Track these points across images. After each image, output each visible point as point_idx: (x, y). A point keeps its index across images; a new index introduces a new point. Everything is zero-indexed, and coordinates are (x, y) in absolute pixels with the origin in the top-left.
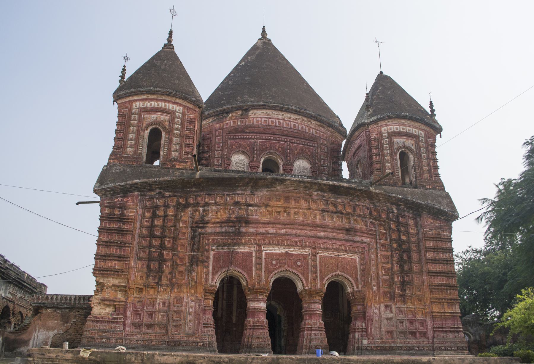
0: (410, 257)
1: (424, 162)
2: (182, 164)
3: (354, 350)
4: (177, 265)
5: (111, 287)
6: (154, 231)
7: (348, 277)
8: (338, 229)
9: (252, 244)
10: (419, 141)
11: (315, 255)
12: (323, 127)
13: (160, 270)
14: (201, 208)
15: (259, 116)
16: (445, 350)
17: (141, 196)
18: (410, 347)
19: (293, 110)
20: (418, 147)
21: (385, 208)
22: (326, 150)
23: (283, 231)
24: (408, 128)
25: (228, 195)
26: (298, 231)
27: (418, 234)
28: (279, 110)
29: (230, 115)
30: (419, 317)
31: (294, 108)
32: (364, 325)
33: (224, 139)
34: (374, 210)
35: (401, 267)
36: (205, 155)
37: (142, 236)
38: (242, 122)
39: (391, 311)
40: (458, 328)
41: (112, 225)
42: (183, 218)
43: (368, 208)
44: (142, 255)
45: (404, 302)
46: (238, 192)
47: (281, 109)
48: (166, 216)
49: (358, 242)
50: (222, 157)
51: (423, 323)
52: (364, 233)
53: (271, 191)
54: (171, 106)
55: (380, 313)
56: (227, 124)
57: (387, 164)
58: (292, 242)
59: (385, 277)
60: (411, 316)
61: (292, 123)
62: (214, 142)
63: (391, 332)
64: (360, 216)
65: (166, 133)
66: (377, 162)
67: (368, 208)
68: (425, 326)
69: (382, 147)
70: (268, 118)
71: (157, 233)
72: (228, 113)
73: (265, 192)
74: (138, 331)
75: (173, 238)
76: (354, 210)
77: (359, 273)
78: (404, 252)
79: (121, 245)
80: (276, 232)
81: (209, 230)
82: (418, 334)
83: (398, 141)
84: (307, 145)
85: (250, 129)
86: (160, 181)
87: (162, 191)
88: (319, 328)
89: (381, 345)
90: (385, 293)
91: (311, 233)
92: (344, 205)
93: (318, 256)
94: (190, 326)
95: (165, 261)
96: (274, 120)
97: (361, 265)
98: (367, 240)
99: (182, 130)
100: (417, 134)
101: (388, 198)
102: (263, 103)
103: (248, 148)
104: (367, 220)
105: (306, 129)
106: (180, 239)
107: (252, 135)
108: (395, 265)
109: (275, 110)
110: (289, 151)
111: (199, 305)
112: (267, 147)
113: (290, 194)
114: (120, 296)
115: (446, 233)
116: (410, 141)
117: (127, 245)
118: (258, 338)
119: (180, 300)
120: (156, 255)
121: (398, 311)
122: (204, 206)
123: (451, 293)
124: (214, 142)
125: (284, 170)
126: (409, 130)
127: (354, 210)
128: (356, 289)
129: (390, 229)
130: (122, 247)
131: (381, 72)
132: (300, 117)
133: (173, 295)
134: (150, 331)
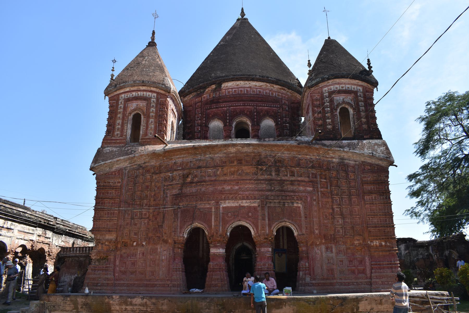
1: (363, 114)
12: (284, 90)
16: (383, 284)
18: (349, 283)
22: (287, 109)
24: (348, 86)
28: (246, 80)
29: (207, 90)
32: (307, 264)
33: (202, 110)
36: (188, 125)
50: (200, 126)
55: (322, 253)
56: (204, 97)
57: (327, 120)
62: (194, 114)
65: (144, 115)
68: (363, 263)
72: (205, 88)
83: (339, 98)
96: (243, 89)
99: (156, 113)
100: (356, 90)
102: (232, 77)
103: (222, 115)
107: (224, 104)
111: (170, 254)
112: (237, 113)
126: (348, 88)
131: (329, 38)
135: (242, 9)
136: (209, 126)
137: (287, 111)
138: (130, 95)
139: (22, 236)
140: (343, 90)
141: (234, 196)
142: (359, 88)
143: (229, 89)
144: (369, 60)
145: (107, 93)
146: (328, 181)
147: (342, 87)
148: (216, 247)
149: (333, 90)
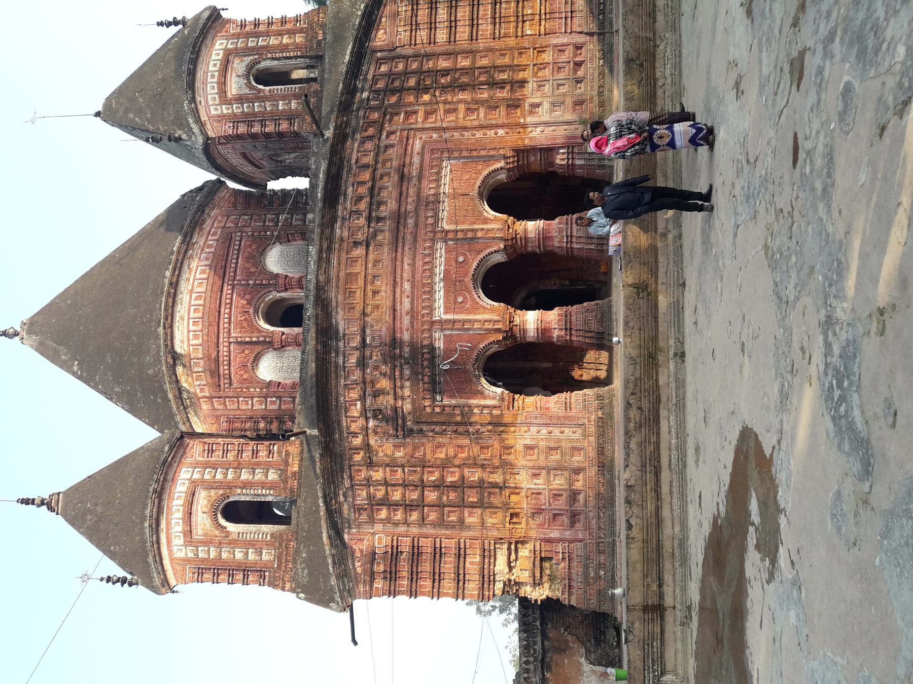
1: (273, 41)
2: (290, 460)
3: (604, 166)
5: (511, 568)
6: (412, 501)
7: (481, 178)
8: (401, 194)
9: (431, 337)
10: (236, 49)
12: (204, 221)
13: (481, 485)
14: (371, 423)
16: (604, 13)
17: (350, 528)
18: (600, 73)
19: (173, 275)
23: (407, 286)
27: (404, 57)
29: (185, 385)
33: (231, 394)
34: (366, 131)
35: (463, 88)
38: (197, 364)
41: (405, 574)
44: (453, 518)
45: (523, 83)
47: (173, 296)
49: (422, 161)
50: (266, 397)
52: (406, 149)
53: (337, 307)
57: (280, 108)
59: (482, 115)
61: (198, 276)
62: (238, 412)
64: (377, 155)
67: (362, 143)
69: (247, 114)
70: (189, 319)
71: (415, 496)
72: (180, 390)
73: (340, 317)
74: (582, 517)
76: (366, 166)
80: (408, 297)
81: (408, 407)
84: (239, 250)
85: (211, 350)
86: (325, 497)
87: (341, 492)
88: (567, 224)
91: (409, 237)
92: (359, 183)
93: (446, 227)
94: (571, 434)
95: (463, 478)
96: (192, 308)
98: (418, 145)
102: (161, 328)
103: (247, 352)
104: (382, 145)
105: (209, 253)
106: (425, 454)
107: (221, 347)
108: (460, 97)
109: (173, 306)
110: (250, 282)
112: (245, 319)
113: (342, 274)
116: (235, 65)
117: (438, 545)
118: (586, 322)
120: (453, 496)
121: (539, 94)
122: (367, 419)
124: (238, 412)
125: (286, 290)
126: (215, 65)
128: (502, 164)
129: (398, 104)
130: (441, 554)
133: (521, 462)
134: (581, 497)
136: (268, 380)
137: (251, 219)
140: (219, 76)
143: (188, 337)
146: (404, 109)
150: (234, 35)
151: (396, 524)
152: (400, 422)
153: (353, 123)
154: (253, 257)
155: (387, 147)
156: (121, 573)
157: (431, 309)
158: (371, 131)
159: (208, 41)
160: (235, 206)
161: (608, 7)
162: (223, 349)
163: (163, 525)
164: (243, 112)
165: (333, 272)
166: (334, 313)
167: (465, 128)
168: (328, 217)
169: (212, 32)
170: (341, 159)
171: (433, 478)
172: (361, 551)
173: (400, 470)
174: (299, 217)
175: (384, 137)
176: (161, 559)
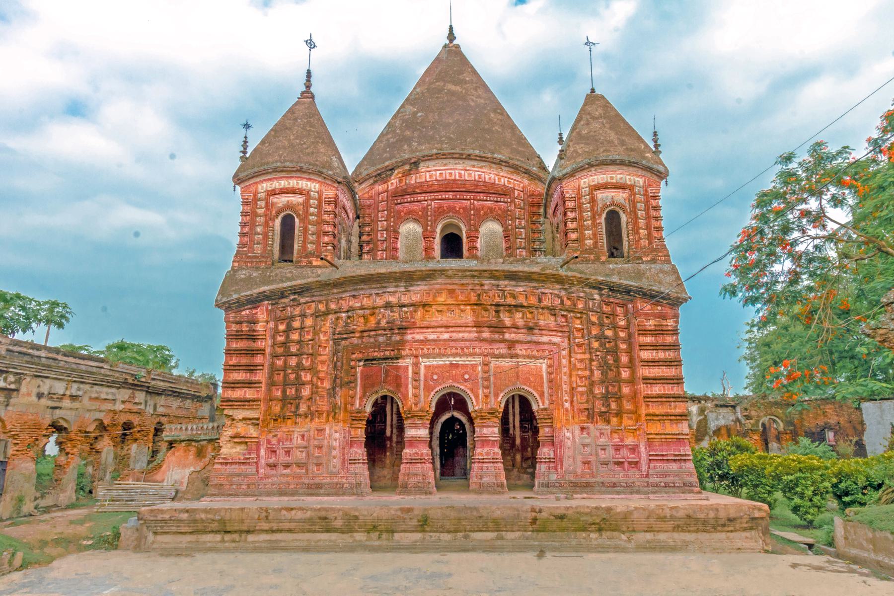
0: (617, 360)
1: (642, 223)
4: (317, 387)
6: (289, 348)
7: (531, 390)
9: (407, 356)
10: (634, 194)
11: (486, 364)
12: (518, 174)
13: (298, 397)
14: (344, 315)
15: (432, 172)
17: (272, 304)
20: (633, 203)
21: (582, 295)
23: (446, 336)
25: (377, 294)
26: (466, 335)
27: (628, 325)
29: (396, 172)
30: (629, 441)
31: (477, 152)
34: (568, 299)
36: (367, 229)
37: (275, 356)
39: (588, 434)
40: (686, 455)
42: (323, 329)
43: (559, 297)
45: (608, 422)
46: (389, 290)
47: (461, 157)
48: (302, 328)
49: (544, 344)
50: (386, 230)
51: (634, 449)
54: (303, 184)
55: (574, 437)
58: (457, 349)
59: (580, 389)
60: (616, 440)
61: (477, 173)
63: (588, 463)
64: (548, 308)
66: (574, 230)
67: (559, 297)
71: (294, 349)
73: (422, 287)
74: (273, 472)
75: (312, 355)
76: (540, 300)
77: (546, 385)
78: (608, 352)
79: (251, 368)
81: (355, 341)
82: (626, 465)
84: (497, 201)
89: (574, 480)
90: (581, 411)
97: (550, 374)
98: (556, 340)
101: (585, 283)
106: (320, 355)
108: (596, 372)
111: (344, 437)
113: (454, 287)
114: (253, 432)
115: (670, 322)
116: (621, 194)
118: (416, 475)
119: (321, 431)
120: (292, 377)
121: (598, 434)
123: (675, 407)
127: (540, 300)
132: (487, 164)
134: (288, 471)
135: (451, 28)
136: (400, 231)
138: (277, 185)
139: (95, 405)
141: (441, 348)
142: (637, 179)
144: (655, 134)
145: (238, 179)
147: (612, 178)
148: (416, 426)
149: (596, 183)
150: (647, 191)
151: (273, 337)
152: (345, 336)
153: (574, 289)
154: (491, 212)
155: (555, 315)
156: (250, 151)
157: (427, 356)
158: (568, 303)
159: (640, 172)
160: (532, 195)
161: (671, 490)
162: (421, 197)
163: (279, 175)
164: (583, 204)
165: (456, 280)
166: (425, 282)
167: (570, 376)
168: (497, 274)
169: (648, 175)
170: (544, 281)
171: (304, 362)
172: (256, 314)
173: (310, 337)
174: (523, 245)
175: (563, 313)
176: (257, 176)
